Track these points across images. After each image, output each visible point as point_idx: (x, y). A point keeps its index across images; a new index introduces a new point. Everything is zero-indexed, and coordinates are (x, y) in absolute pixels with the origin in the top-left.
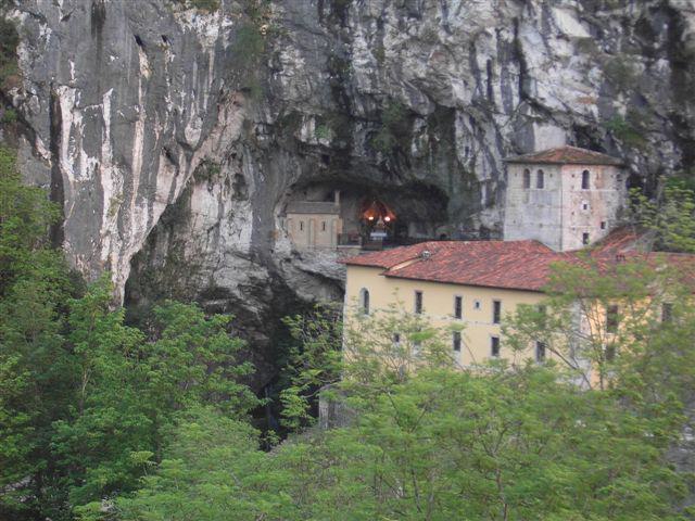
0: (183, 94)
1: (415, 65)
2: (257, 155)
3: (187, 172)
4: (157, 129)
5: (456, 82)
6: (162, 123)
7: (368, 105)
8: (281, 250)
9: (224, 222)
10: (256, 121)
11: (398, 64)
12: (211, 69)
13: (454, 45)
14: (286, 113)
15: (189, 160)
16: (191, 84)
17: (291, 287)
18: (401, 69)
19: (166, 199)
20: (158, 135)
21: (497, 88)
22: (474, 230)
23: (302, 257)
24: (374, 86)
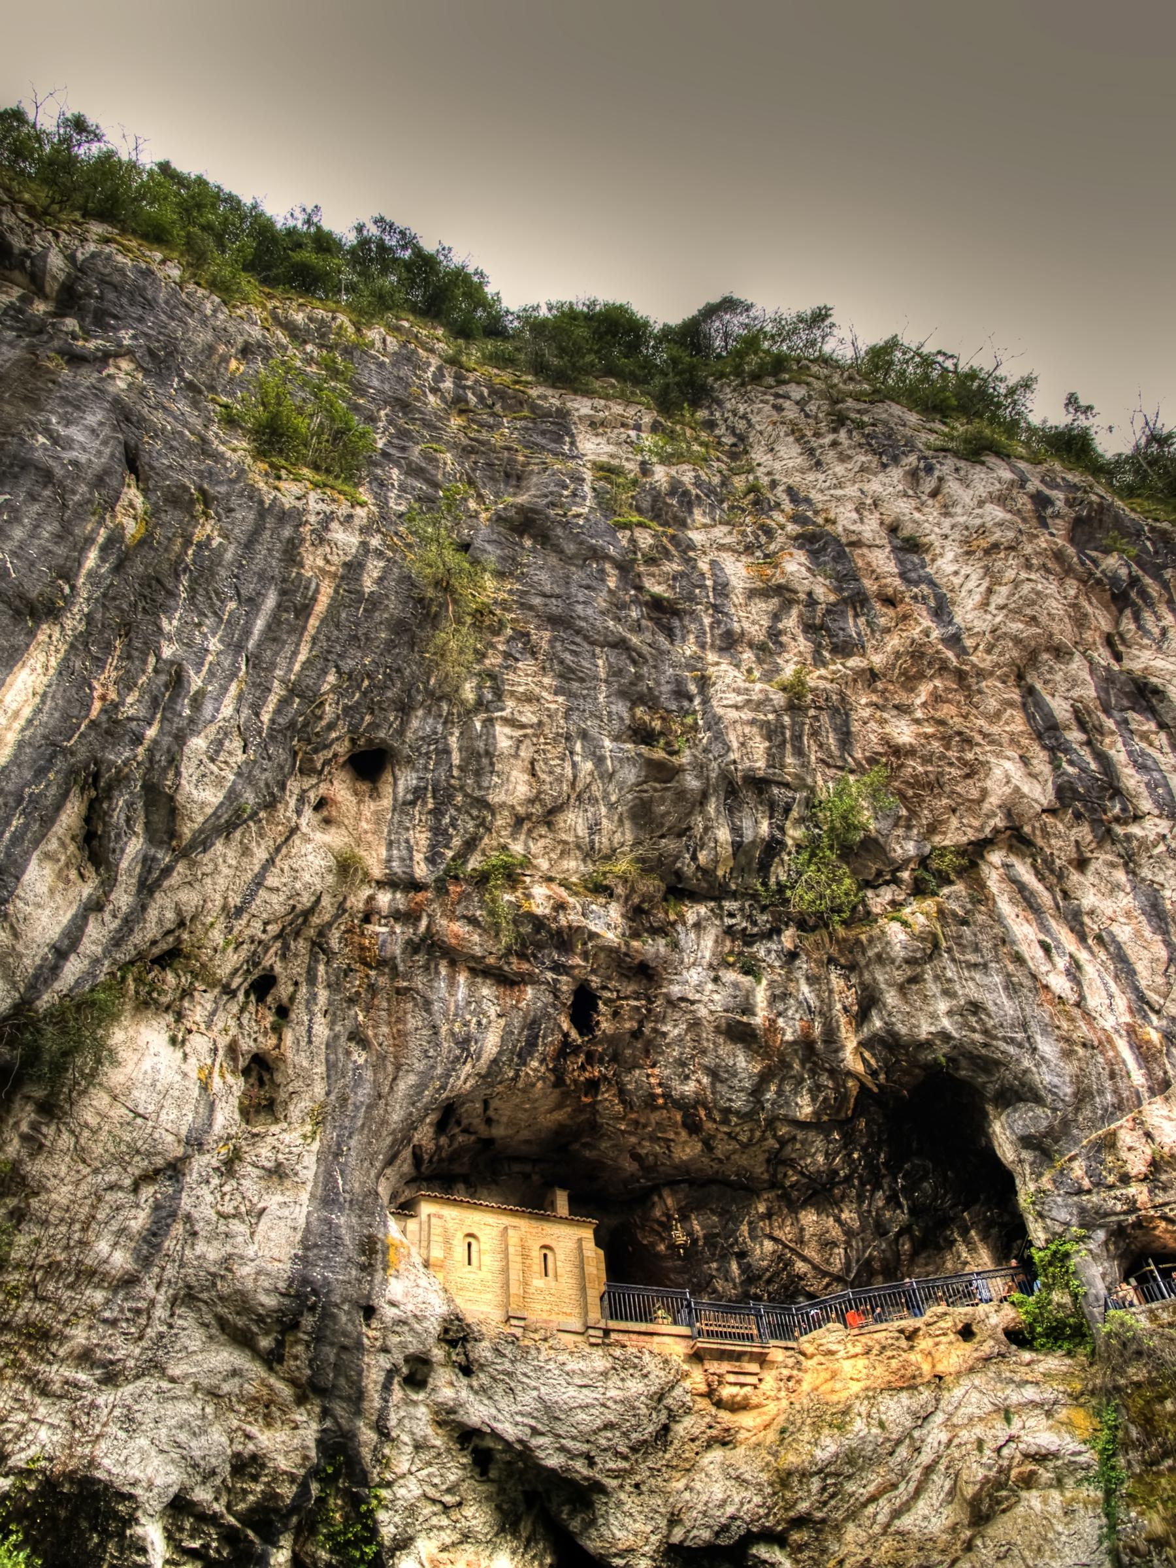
0: (214, 644)
1: (882, 722)
2: (355, 984)
3: (129, 923)
4: (104, 684)
5: (998, 755)
6: (126, 683)
7: (747, 823)
8: (410, 1307)
9: (201, 1163)
10: (377, 872)
11: (841, 712)
12: (313, 622)
13: (981, 674)
14: (474, 863)
15: (147, 888)
16: (247, 633)
17: (388, 1525)
18: (847, 723)
19: (31, 959)
20: (97, 705)
21: (1119, 754)
22: (1125, 1179)
23: (482, 1351)
24: (774, 759)
